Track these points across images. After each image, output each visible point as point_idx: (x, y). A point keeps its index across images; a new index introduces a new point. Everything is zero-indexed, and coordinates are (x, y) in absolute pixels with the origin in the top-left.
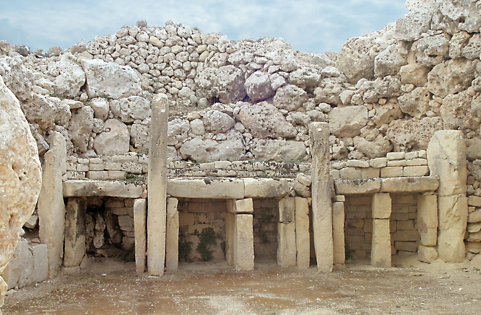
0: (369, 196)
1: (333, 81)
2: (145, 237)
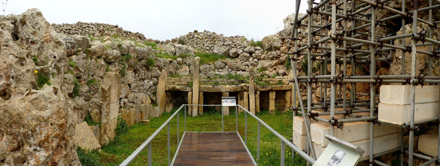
0: (268, 92)
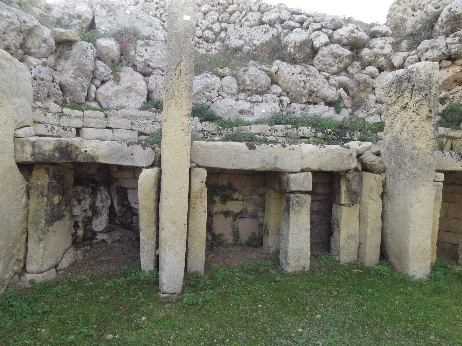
1: (384, 41)
2: (154, 229)
